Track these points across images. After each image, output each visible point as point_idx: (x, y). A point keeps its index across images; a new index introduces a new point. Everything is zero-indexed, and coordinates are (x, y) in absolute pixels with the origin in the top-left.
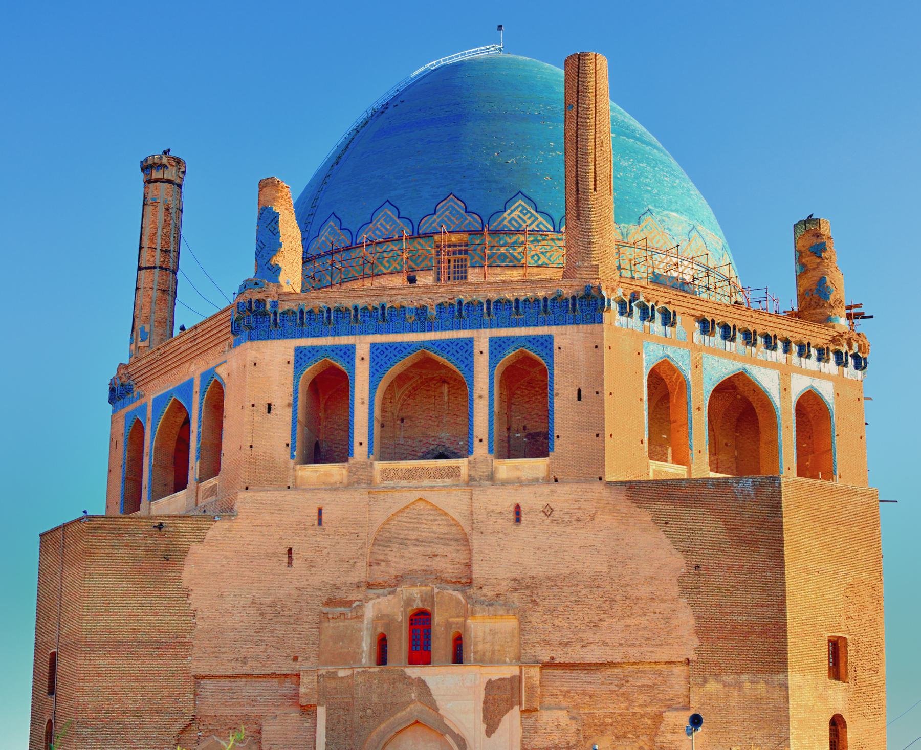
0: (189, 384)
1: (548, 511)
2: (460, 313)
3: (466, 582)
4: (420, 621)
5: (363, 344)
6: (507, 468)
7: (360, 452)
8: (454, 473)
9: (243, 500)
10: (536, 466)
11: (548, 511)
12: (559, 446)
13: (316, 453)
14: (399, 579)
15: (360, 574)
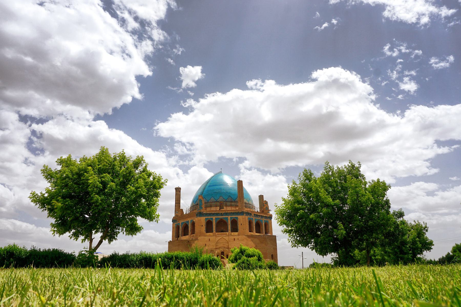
0: (188, 221)
1: (238, 239)
2: (226, 214)
3: (228, 248)
4: (223, 253)
5: (214, 218)
6: (233, 233)
7: (214, 231)
8: (226, 234)
9: (199, 238)
10: (236, 233)
11: (238, 239)
12: (239, 231)
13: (207, 231)
14: (220, 248)
15: (215, 247)
